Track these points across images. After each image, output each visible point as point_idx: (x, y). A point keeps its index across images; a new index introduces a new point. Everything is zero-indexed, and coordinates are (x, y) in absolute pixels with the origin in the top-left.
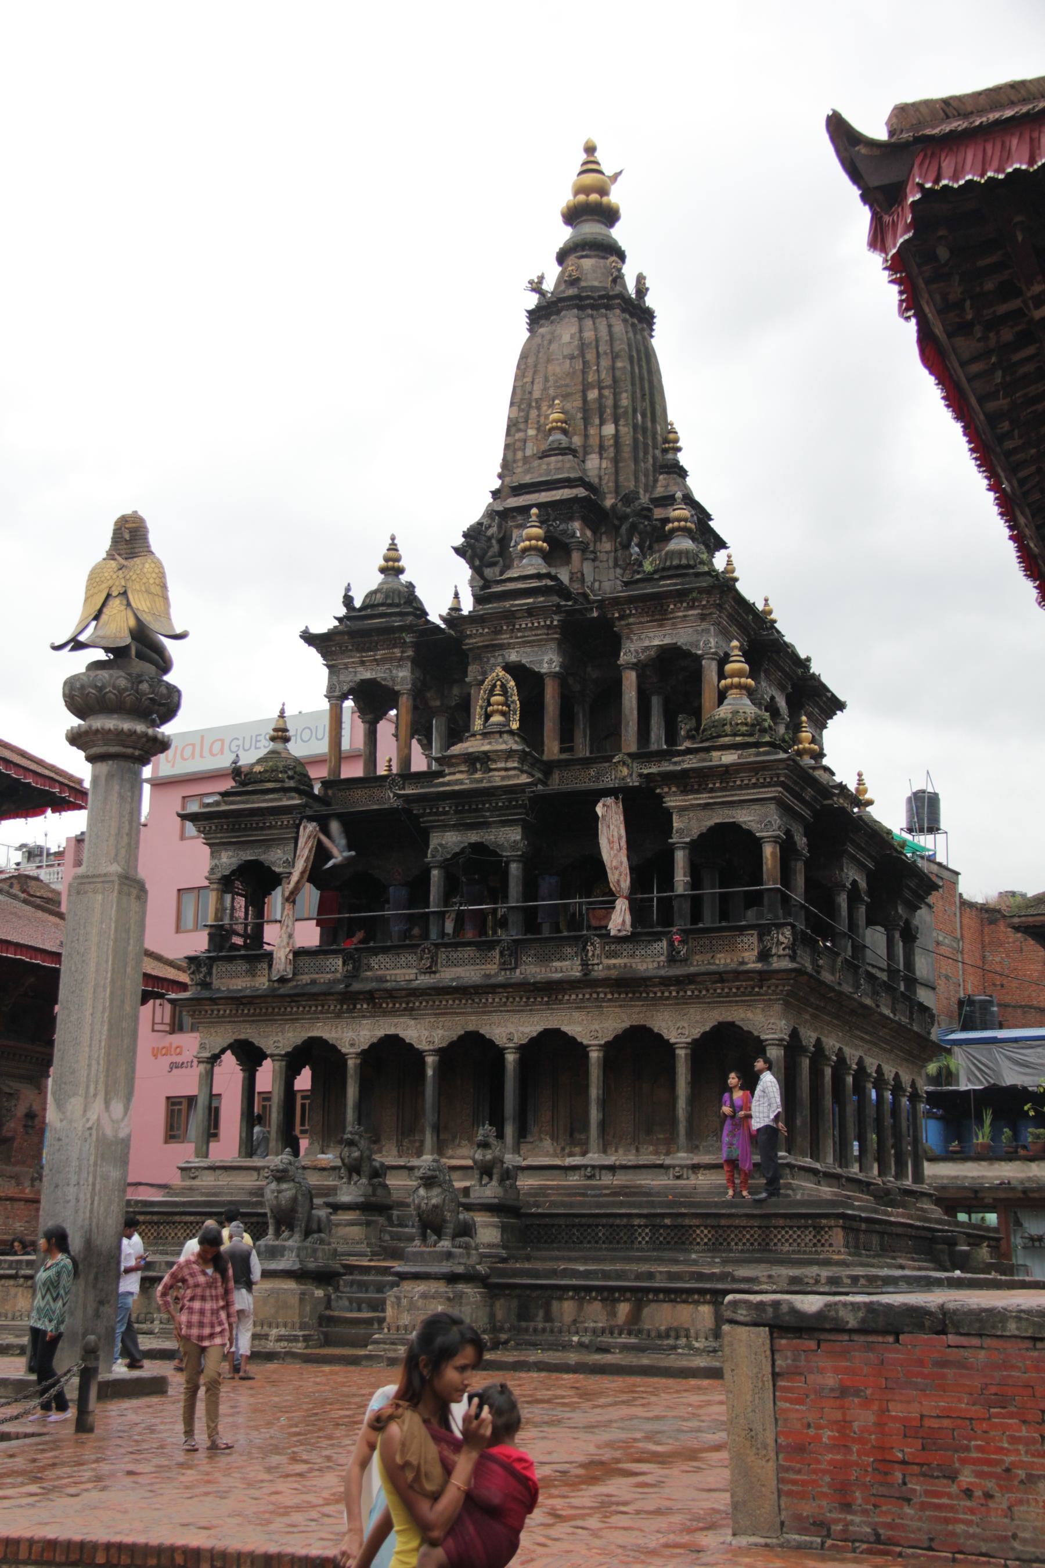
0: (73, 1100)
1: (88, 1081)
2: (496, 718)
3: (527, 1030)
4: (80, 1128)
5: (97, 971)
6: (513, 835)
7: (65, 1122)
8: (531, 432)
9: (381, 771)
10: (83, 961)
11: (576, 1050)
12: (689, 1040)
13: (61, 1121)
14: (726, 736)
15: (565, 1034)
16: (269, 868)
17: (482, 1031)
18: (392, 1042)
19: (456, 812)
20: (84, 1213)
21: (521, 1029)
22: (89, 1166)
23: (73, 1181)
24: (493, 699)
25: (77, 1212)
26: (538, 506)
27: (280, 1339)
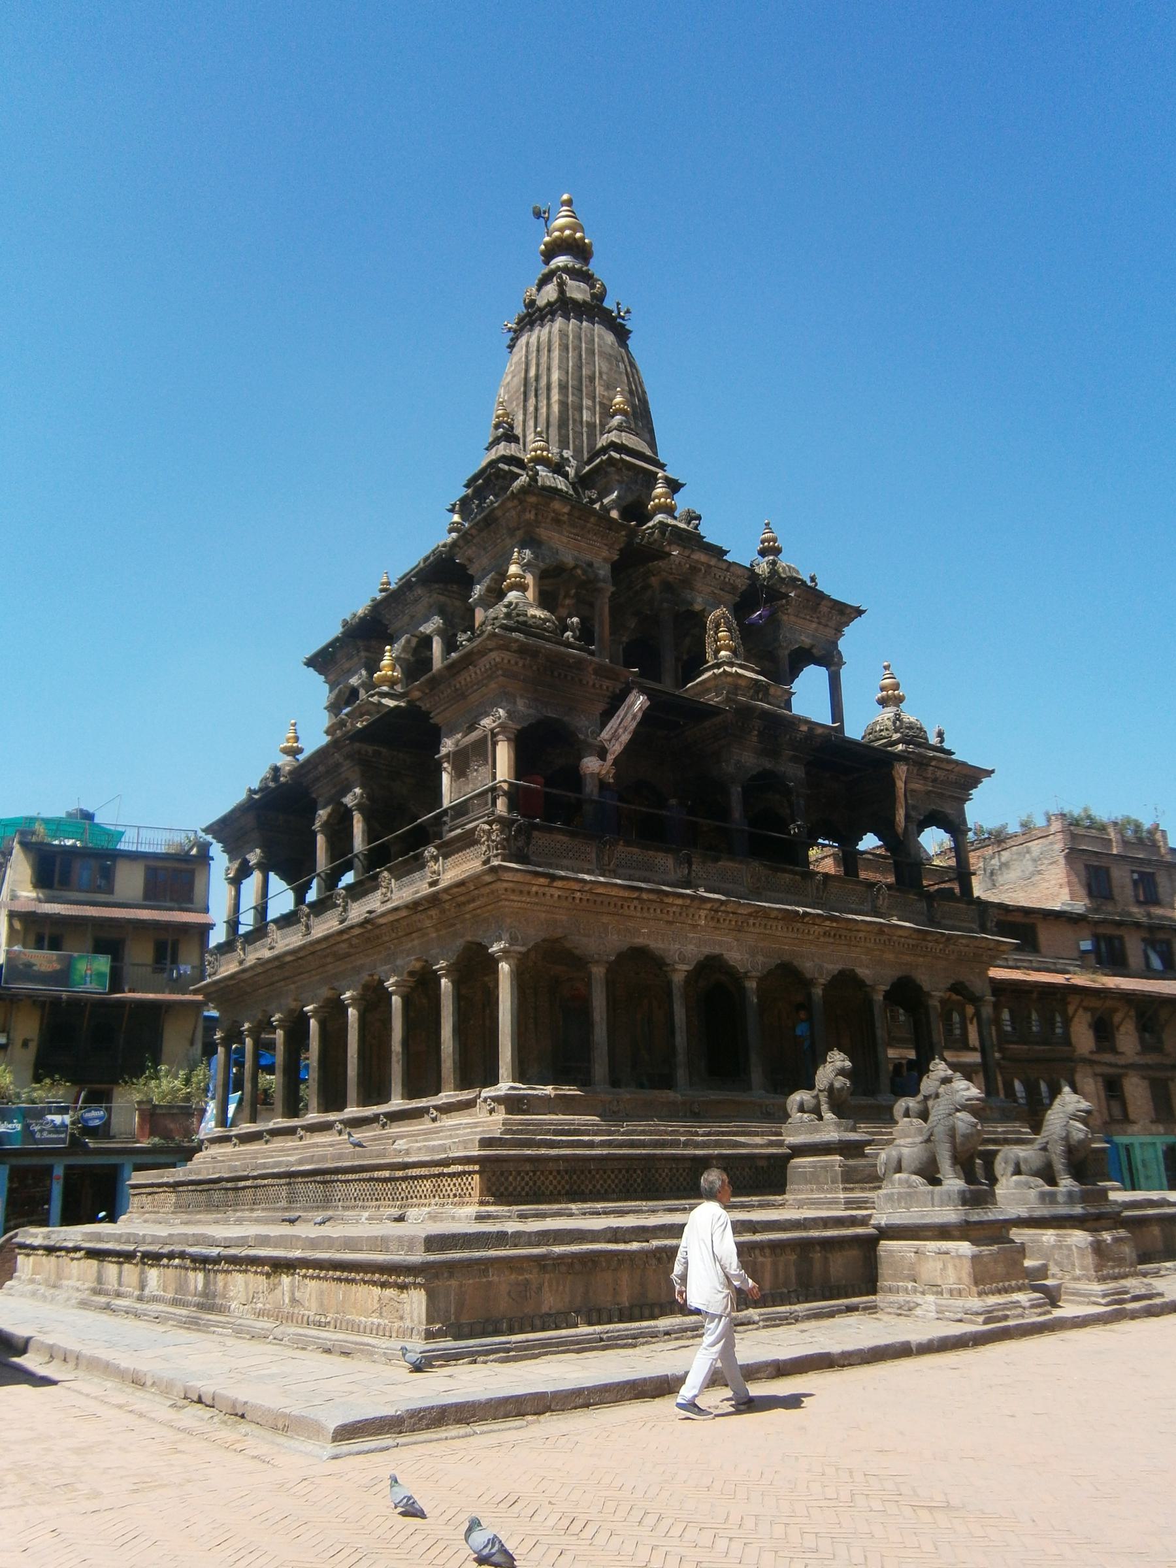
2: (723, 653)
3: (830, 967)
15: (856, 975)
17: (795, 963)
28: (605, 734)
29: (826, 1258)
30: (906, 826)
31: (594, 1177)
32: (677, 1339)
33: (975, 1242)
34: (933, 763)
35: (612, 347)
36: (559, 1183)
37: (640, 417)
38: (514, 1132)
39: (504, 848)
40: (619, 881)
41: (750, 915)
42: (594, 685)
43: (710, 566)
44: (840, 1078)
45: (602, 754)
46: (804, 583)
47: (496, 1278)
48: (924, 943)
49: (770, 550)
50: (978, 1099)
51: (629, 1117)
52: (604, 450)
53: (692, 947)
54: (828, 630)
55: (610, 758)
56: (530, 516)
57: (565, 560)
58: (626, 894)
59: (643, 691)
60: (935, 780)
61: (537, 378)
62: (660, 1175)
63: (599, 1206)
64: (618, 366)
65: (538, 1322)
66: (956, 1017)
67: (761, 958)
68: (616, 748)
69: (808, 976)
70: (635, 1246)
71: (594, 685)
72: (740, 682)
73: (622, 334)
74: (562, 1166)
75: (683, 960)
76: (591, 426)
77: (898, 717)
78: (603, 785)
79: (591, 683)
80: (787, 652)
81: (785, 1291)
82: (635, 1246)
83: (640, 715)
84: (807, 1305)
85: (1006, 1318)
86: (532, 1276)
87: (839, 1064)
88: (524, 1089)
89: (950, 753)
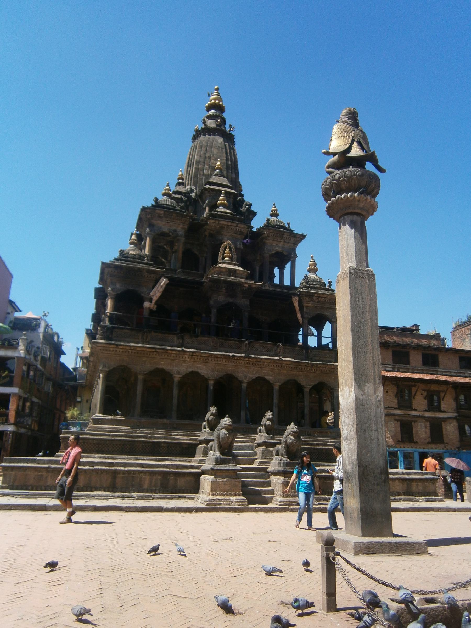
0: (367, 384)
1: (375, 376)
3: (251, 376)
4: (373, 398)
5: (371, 318)
6: (247, 302)
7: (364, 396)
8: (206, 167)
9: (172, 268)
10: (363, 312)
11: (269, 384)
12: (311, 387)
13: (362, 395)
14: (319, 285)
17: (234, 374)
18: (195, 374)
20: (383, 446)
21: (249, 375)
22: (382, 421)
23: (374, 428)
24: (226, 251)
25: (378, 445)
26: (225, 191)
28: (151, 294)
29: (176, 480)
30: (303, 321)
31: (108, 446)
33: (215, 476)
34: (316, 295)
35: (220, 144)
36: (94, 447)
37: (231, 169)
39: (102, 335)
40: (148, 346)
41: (208, 357)
42: (148, 276)
43: (228, 225)
44: (212, 416)
45: (151, 300)
47: (29, 473)
48: (300, 367)
50: (227, 425)
51: (144, 428)
54: (289, 244)
55: (154, 302)
56: (149, 216)
57: (164, 230)
58: (150, 350)
59: (166, 277)
60: (319, 302)
61: (192, 159)
62: (137, 447)
63: (107, 456)
64: (222, 151)
65: (43, 488)
66: (435, 398)
67: (217, 373)
68: (155, 299)
69: (240, 379)
71: (148, 276)
72: (222, 270)
74: (95, 442)
75: (178, 373)
76: (207, 176)
78: (151, 311)
79: (146, 276)
80: (268, 255)
81: (155, 488)
82: (87, 467)
83: (164, 286)
84: (158, 494)
85: (220, 504)
86: (44, 473)
87: (212, 411)
88: (101, 416)
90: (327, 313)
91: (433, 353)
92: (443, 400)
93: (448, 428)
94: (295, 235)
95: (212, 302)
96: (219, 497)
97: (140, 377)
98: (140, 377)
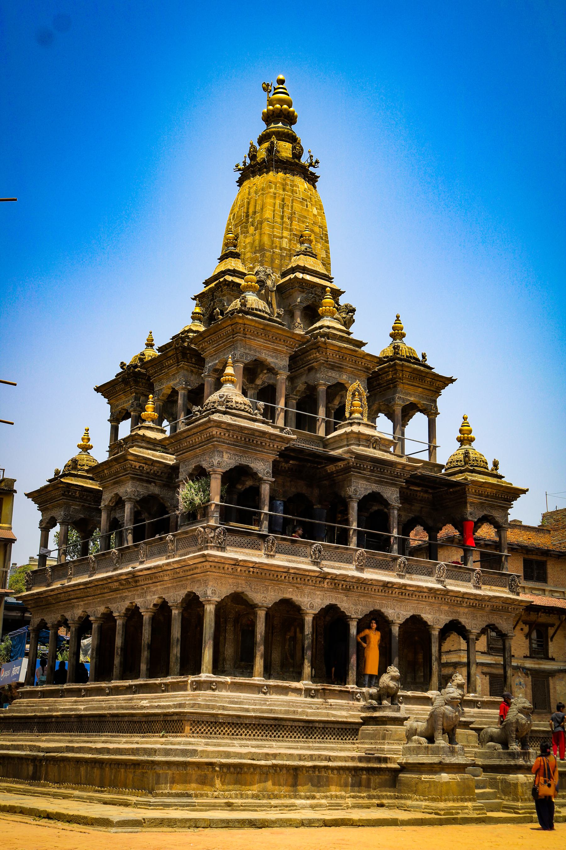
3: (405, 613)
15: (422, 618)
16: (256, 474)
17: (383, 610)
19: (372, 471)
27: (475, 809)
32: (280, 810)
38: (207, 701)
46: (417, 359)
49: (397, 334)
52: (293, 270)
53: (319, 600)
61: (255, 213)
70: (263, 763)
73: (312, 179)
75: (312, 607)
77: (466, 454)
85: (458, 813)
89: (501, 477)
90: (496, 514)
91: (539, 558)
92: (552, 641)
93: (558, 688)
94: (437, 377)
95: (350, 491)
96: (450, 804)
97: (261, 614)
98: (261, 614)
